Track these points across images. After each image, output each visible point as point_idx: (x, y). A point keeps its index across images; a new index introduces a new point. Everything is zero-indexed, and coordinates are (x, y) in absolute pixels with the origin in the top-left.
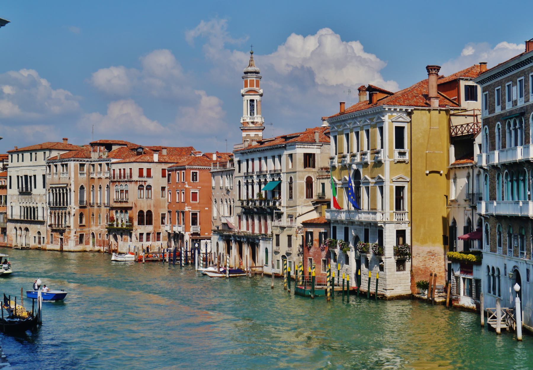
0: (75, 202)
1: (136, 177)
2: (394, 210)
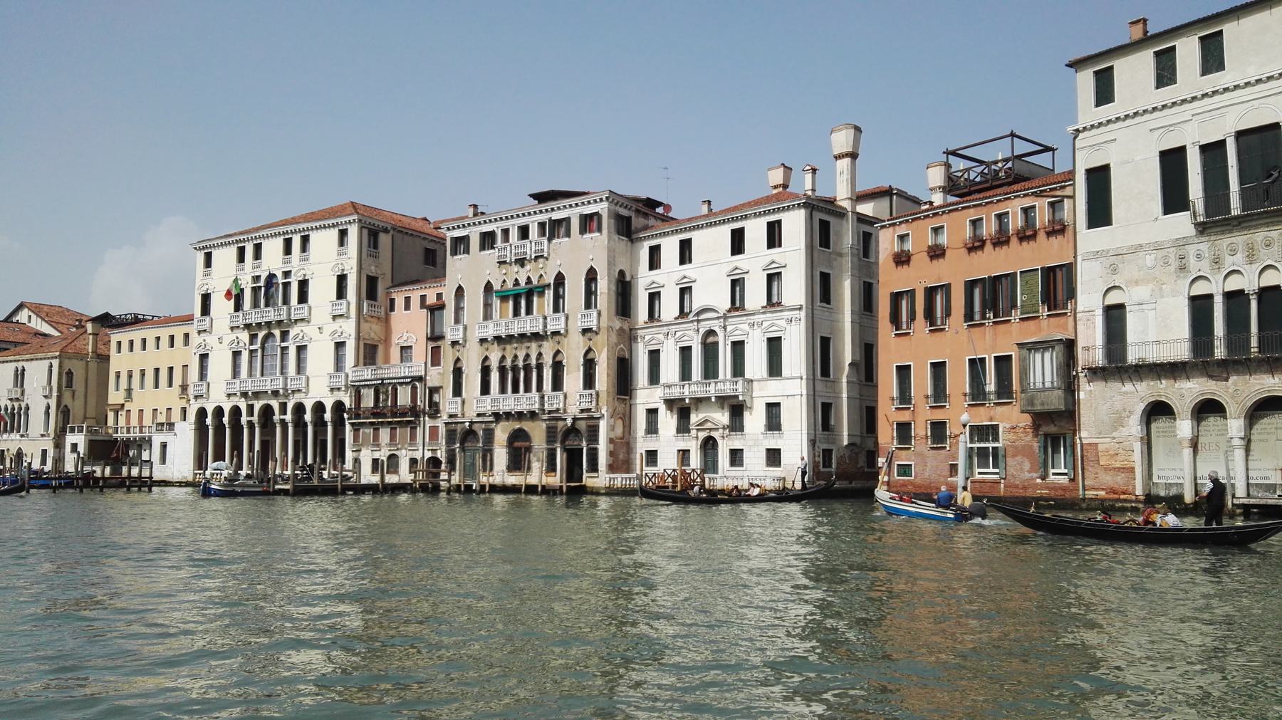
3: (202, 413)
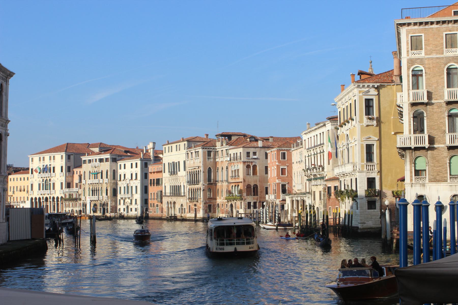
0: (204, 180)
1: (244, 158)
2: (365, 162)
3: (32, 199)
